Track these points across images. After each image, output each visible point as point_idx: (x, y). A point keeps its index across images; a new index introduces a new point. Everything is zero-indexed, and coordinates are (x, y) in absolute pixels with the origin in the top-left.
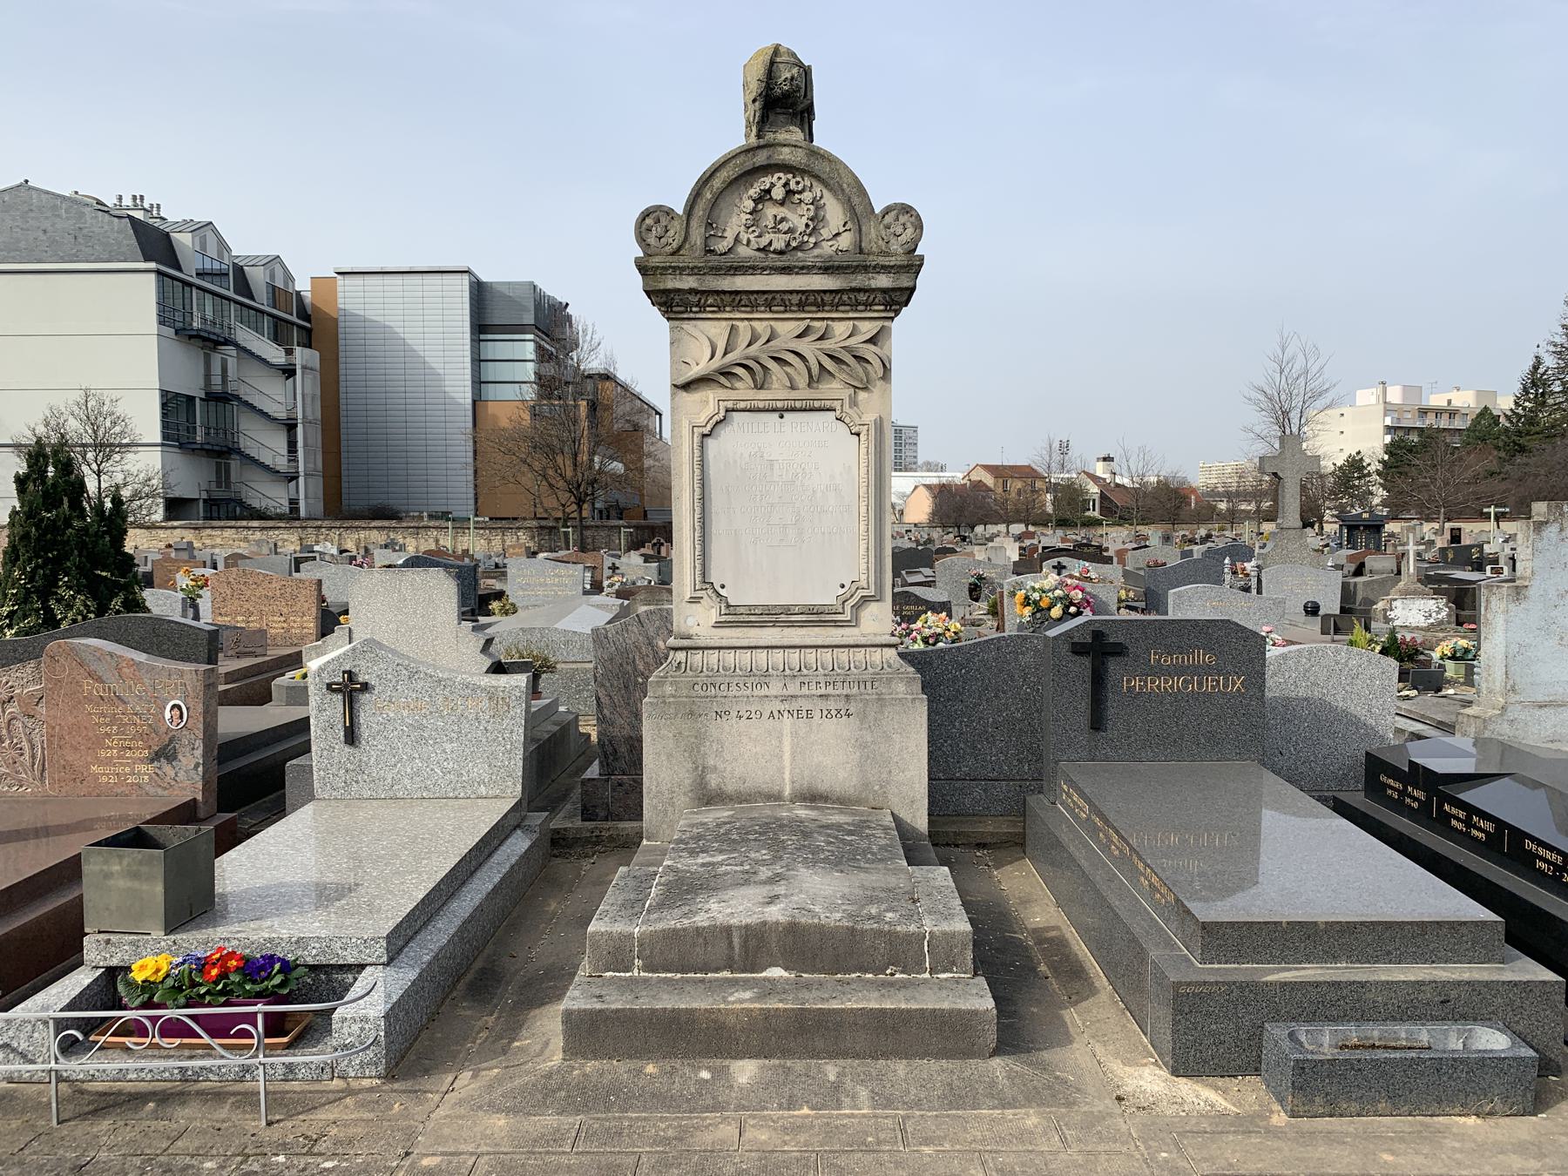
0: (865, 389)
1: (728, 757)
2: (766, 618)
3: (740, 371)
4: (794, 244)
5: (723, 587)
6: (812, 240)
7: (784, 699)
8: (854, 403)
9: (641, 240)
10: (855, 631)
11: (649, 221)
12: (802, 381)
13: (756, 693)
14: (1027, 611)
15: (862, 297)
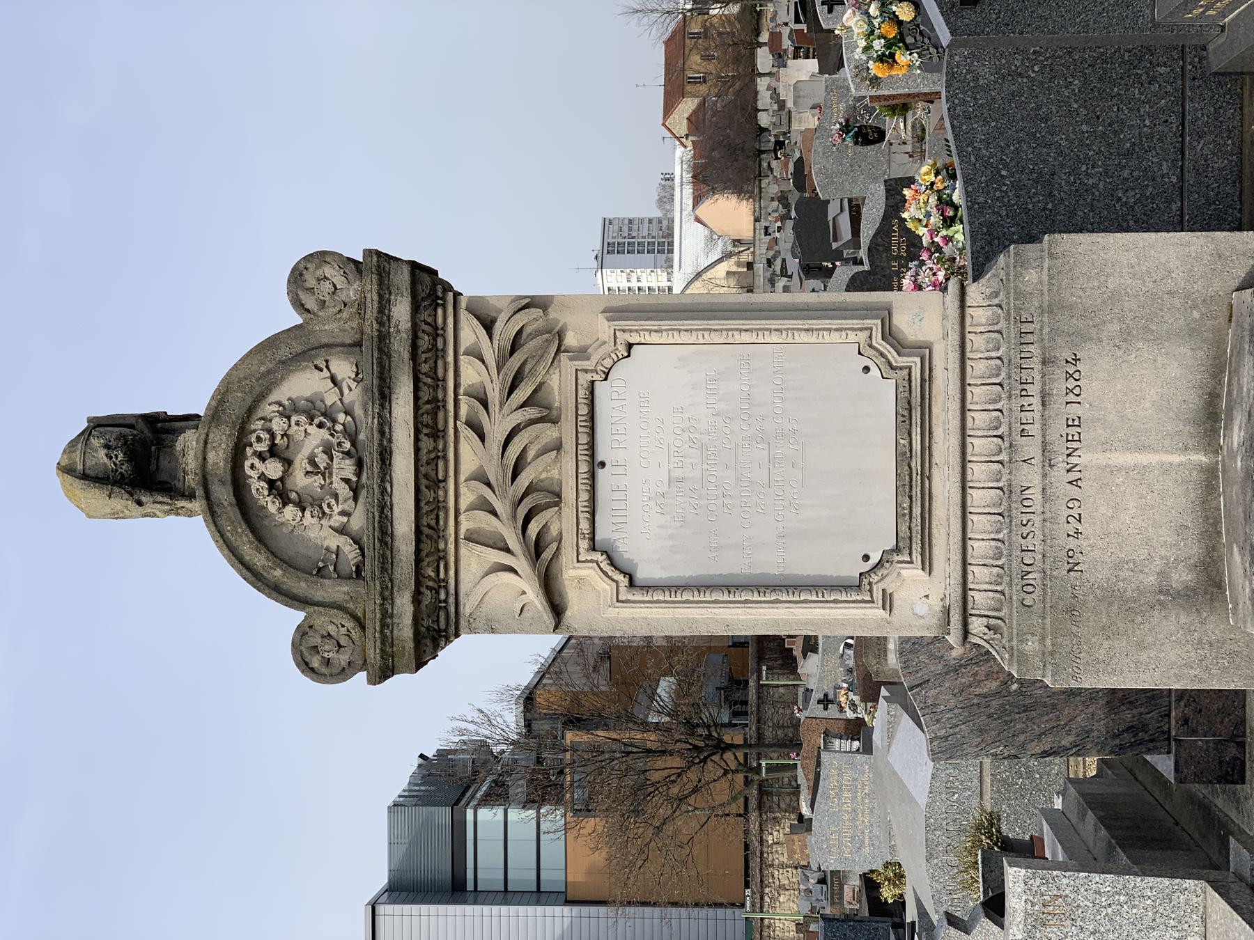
0: (560, 335)
1: (1143, 553)
2: (917, 490)
3: (534, 528)
4: (347, 445)
5: (866, 558)
6: (341, 417)
7: (1048, 463)
8: (582, 353)
9: (342, 674)
10: (938, 351)
11: (315, 663)
12: (548, 433)
13: (1037, 507)
14: (902, 58)
15: (425, 341)
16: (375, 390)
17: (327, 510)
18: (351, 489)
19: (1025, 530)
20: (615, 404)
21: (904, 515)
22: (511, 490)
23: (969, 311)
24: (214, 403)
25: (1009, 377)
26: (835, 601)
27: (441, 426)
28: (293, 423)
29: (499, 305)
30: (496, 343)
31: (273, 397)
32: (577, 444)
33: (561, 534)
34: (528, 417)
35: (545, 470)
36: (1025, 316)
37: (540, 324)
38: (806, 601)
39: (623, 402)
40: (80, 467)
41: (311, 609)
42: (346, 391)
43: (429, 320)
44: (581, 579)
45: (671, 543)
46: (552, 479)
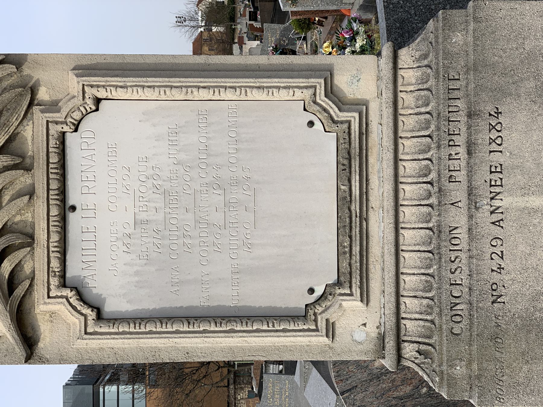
0: (33, 91)
2: (356, 231)
5: (311, 291)
7: (473, 204)
8: (53, 106)
10: (374, 107)
12: (23, 180)
13: (464, 245)
19: (454, 266)
20: (86, 154)
21: (345, 253)
23: (401, 72)
25: (438, 129)
26: (284, 330)
32: (48, 190)
33: (34, 272)
35: (19, 213)
36: (453, 74)
38: (257, 331)
39: (92, 152)
44: (52, 314)
45: (136, 279)
46: (25, 222)
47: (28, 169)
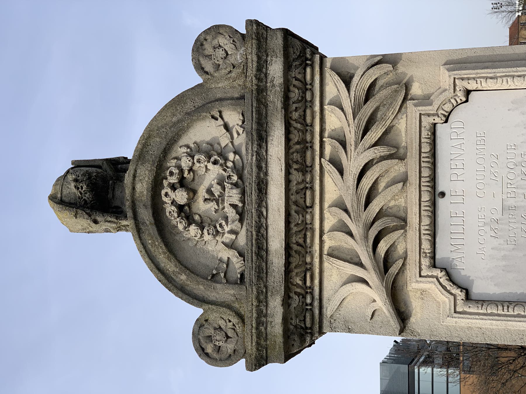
0: (407, 87)
3: (383, 247)
4: (235, 178)
8: (426, 100)
9: (228, 360)
11: (209, 349)
12: (396, 168)
15: (295, 94)
16: (254, 133)
17: (219, 229)
18: (237, 213)
20: (455, 143)
22: (364, 215)
24: (140, 146)
27: (308, 163)
28: (195, 161)
29: (356, 63)
30: (352, 93)
31: (184, 141)
32: (420, 177)
33: (406, 252)
34: (378, 155)
35: (393, 198)
37: (390, 77)
39: (462, 141)
40: (59, 196)
41: (207, 307)
42: (235, 135)
43: (299, 76)
44: (423, 292)
45: (504, 263)
46: (398, 207)
47: (402, 159)
